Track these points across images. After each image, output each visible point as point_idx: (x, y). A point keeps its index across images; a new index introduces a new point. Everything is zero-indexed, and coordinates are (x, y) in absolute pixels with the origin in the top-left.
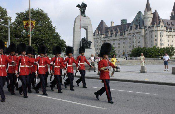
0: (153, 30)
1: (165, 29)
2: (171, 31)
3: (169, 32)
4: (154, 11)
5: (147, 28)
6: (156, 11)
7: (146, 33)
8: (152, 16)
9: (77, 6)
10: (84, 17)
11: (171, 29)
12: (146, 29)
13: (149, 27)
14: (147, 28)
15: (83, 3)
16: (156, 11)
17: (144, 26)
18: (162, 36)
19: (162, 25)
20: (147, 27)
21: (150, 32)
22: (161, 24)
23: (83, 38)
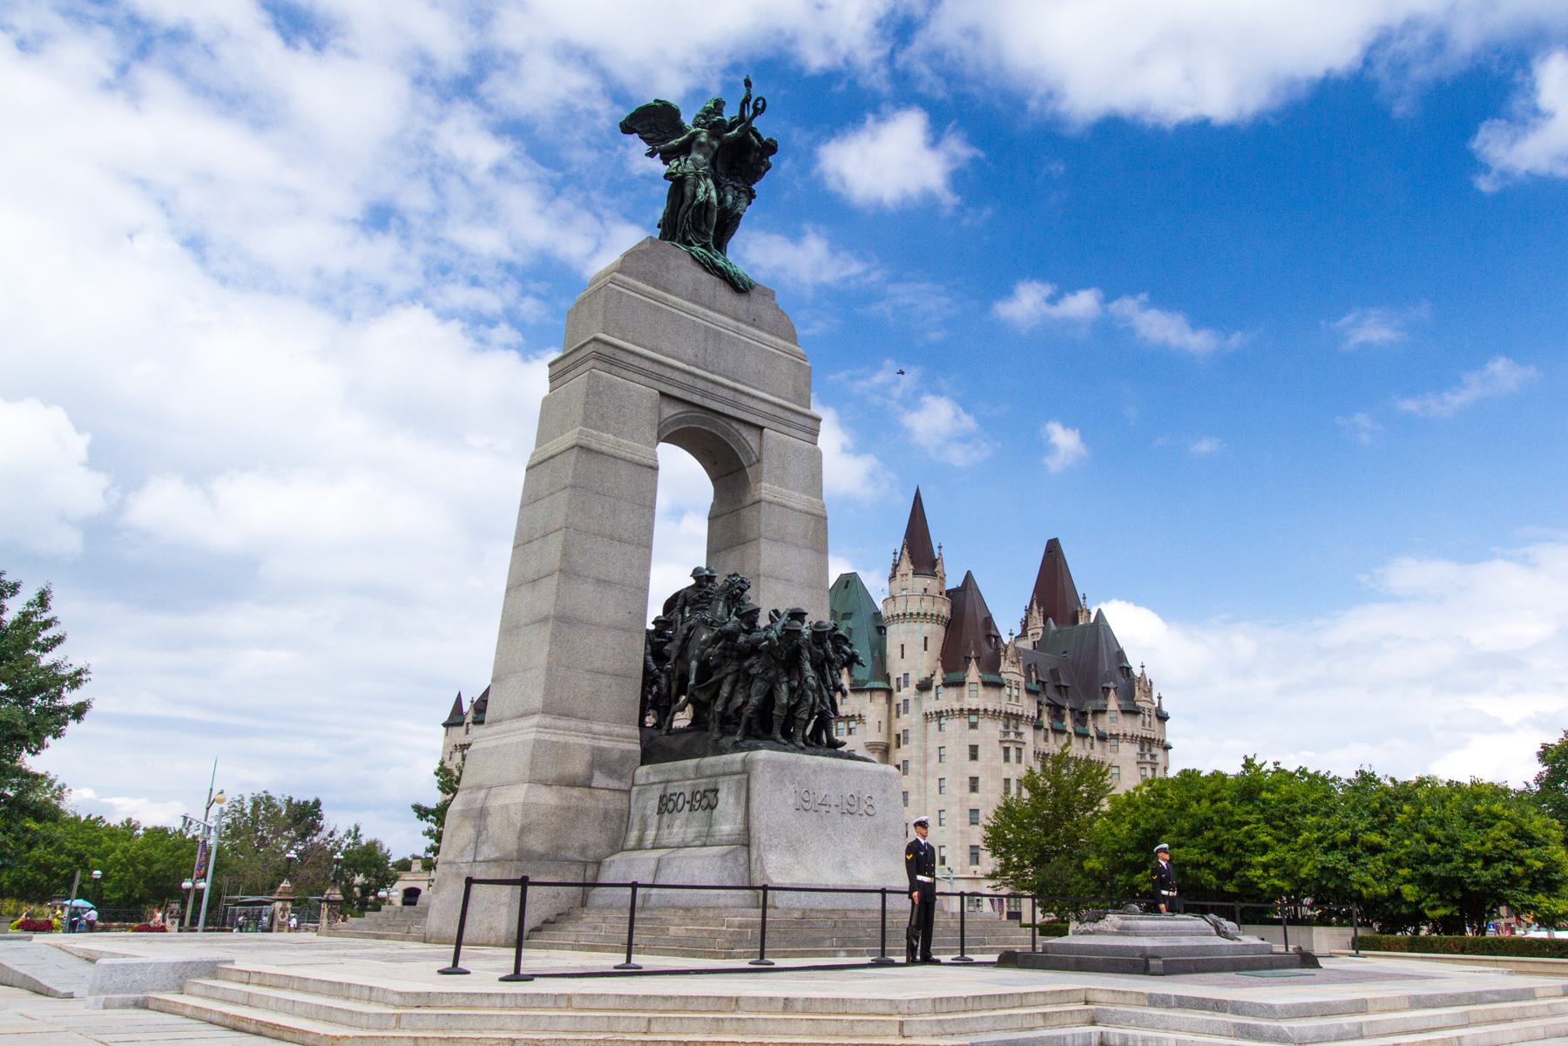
0: (957, 706)
1: (1028, 706)
2: (1057, 725)
3: (1051, 736)
4: (954, 581)
5: (908, 692)
6: (969, 576)
7: (899, 725)
8: (945, 610)
10: (724, 294)
11: (1057, 712)
12: (899, 697)
13: (924, 686)
14: (908, 692)
16: (969, 576)
17: (887, 678)
18: (1013, 753)
19: (1018, 678)
20: (912, 688)
21: (933, 725)
22: (1010, 671)
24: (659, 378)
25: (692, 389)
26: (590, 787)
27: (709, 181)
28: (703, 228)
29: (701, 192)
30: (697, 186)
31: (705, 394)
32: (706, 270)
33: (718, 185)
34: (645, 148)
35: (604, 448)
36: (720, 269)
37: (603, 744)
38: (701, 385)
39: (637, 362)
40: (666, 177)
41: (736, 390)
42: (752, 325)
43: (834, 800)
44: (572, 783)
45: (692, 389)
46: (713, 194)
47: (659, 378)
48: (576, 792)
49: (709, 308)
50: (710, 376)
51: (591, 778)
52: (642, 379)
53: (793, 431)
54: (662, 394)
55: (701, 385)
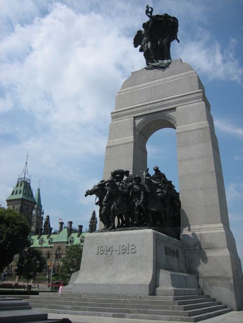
9: (136, 46)
24: (133, 113)
25: (145, 110)
31: (150, 109)
32: (152, 69)
35: (115, 144)
36: (155, 66)
38: (147, 107)
39: (124, 112)
42: (171, 75)
43: (115, 248)
45: (145, 110)
47: (133, 113)
49: (154, 80)
52: (127, 116)
53: (189, 102)
54: (134, 117)
55: (147, 107)
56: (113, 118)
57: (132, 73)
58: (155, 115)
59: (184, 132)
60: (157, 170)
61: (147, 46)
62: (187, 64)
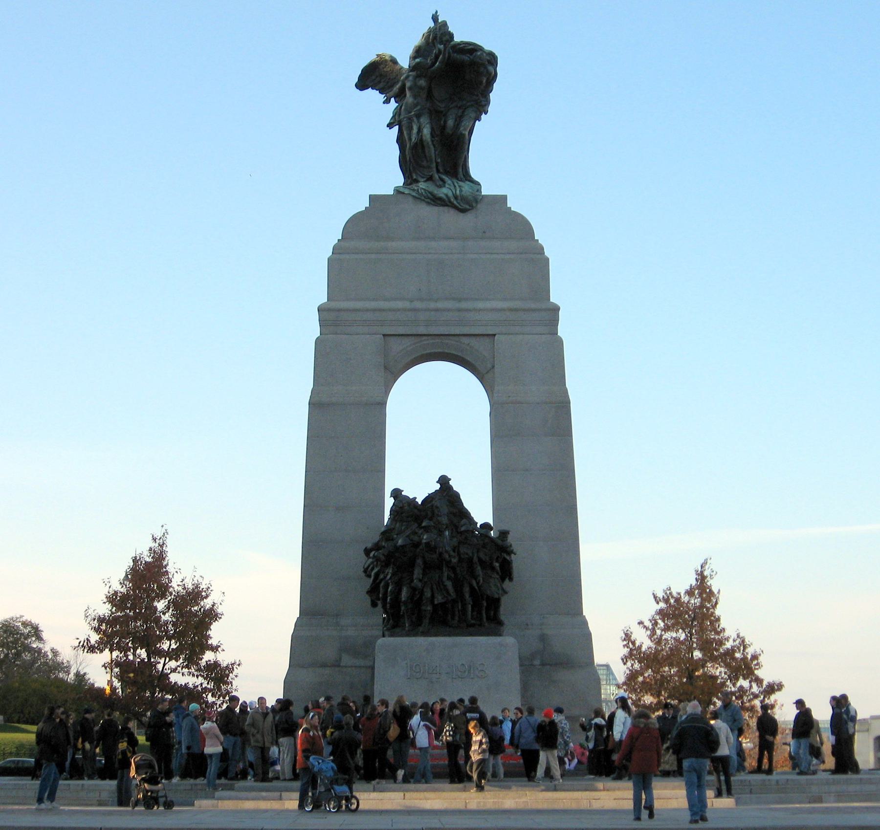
15: (439, 34)
23: (420, 489)
26: (339, 666)
27: (425, 120)
28: (425, 163)
29: (415, 130)
30: (410, 129)
32: (428, 203)
33: (437, 116)
34: (382, 98)
36: (440, 199)
37: (351, 632)
40: (390, 126)
41: (459, 310)
44: (324, 665)
46: (426, 131)
48: (327, 671)
49: (433, 239)
50: (432, 305)
51: (340, 659)
54: (384, 335)
56: (323, 323)
57: (372, 198)
58: (437, 340)
59: (512, 403)
60: (444, 481)
61: (420, 130)
62: (523, 217)
